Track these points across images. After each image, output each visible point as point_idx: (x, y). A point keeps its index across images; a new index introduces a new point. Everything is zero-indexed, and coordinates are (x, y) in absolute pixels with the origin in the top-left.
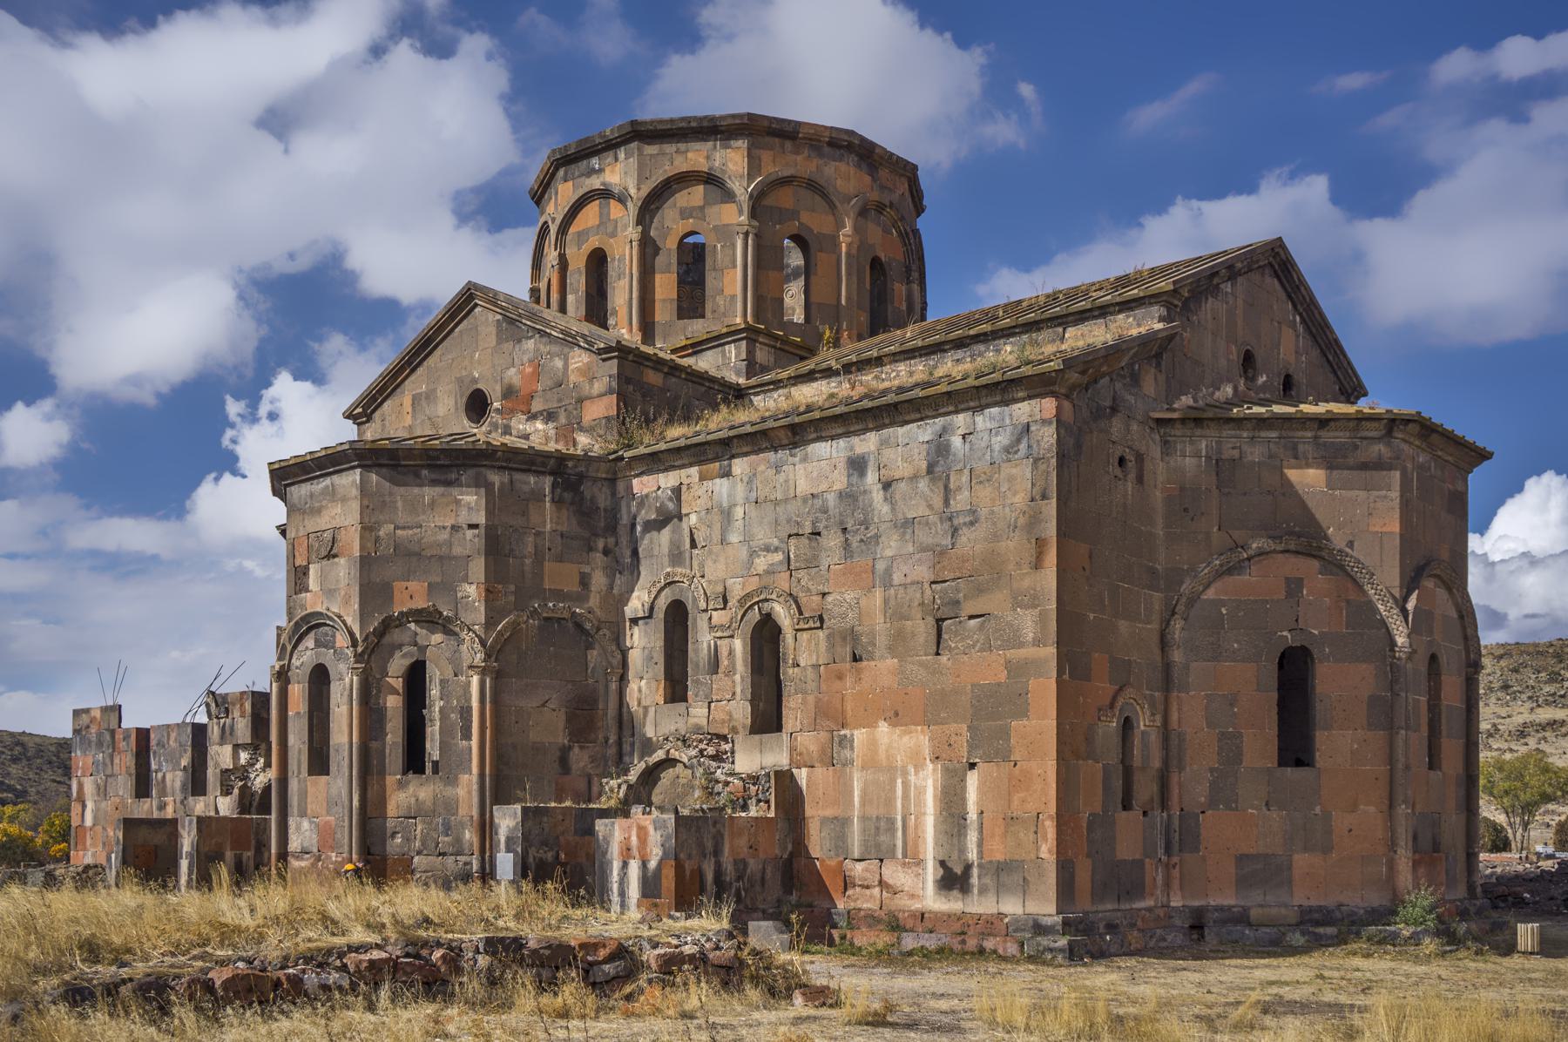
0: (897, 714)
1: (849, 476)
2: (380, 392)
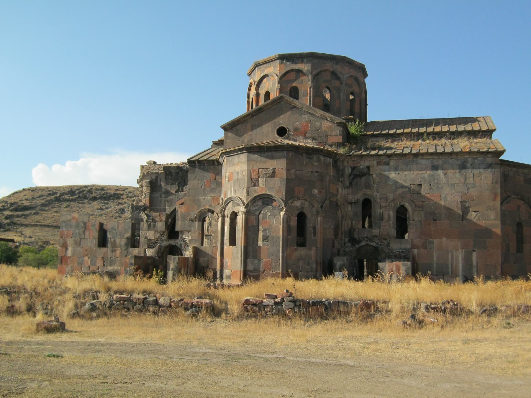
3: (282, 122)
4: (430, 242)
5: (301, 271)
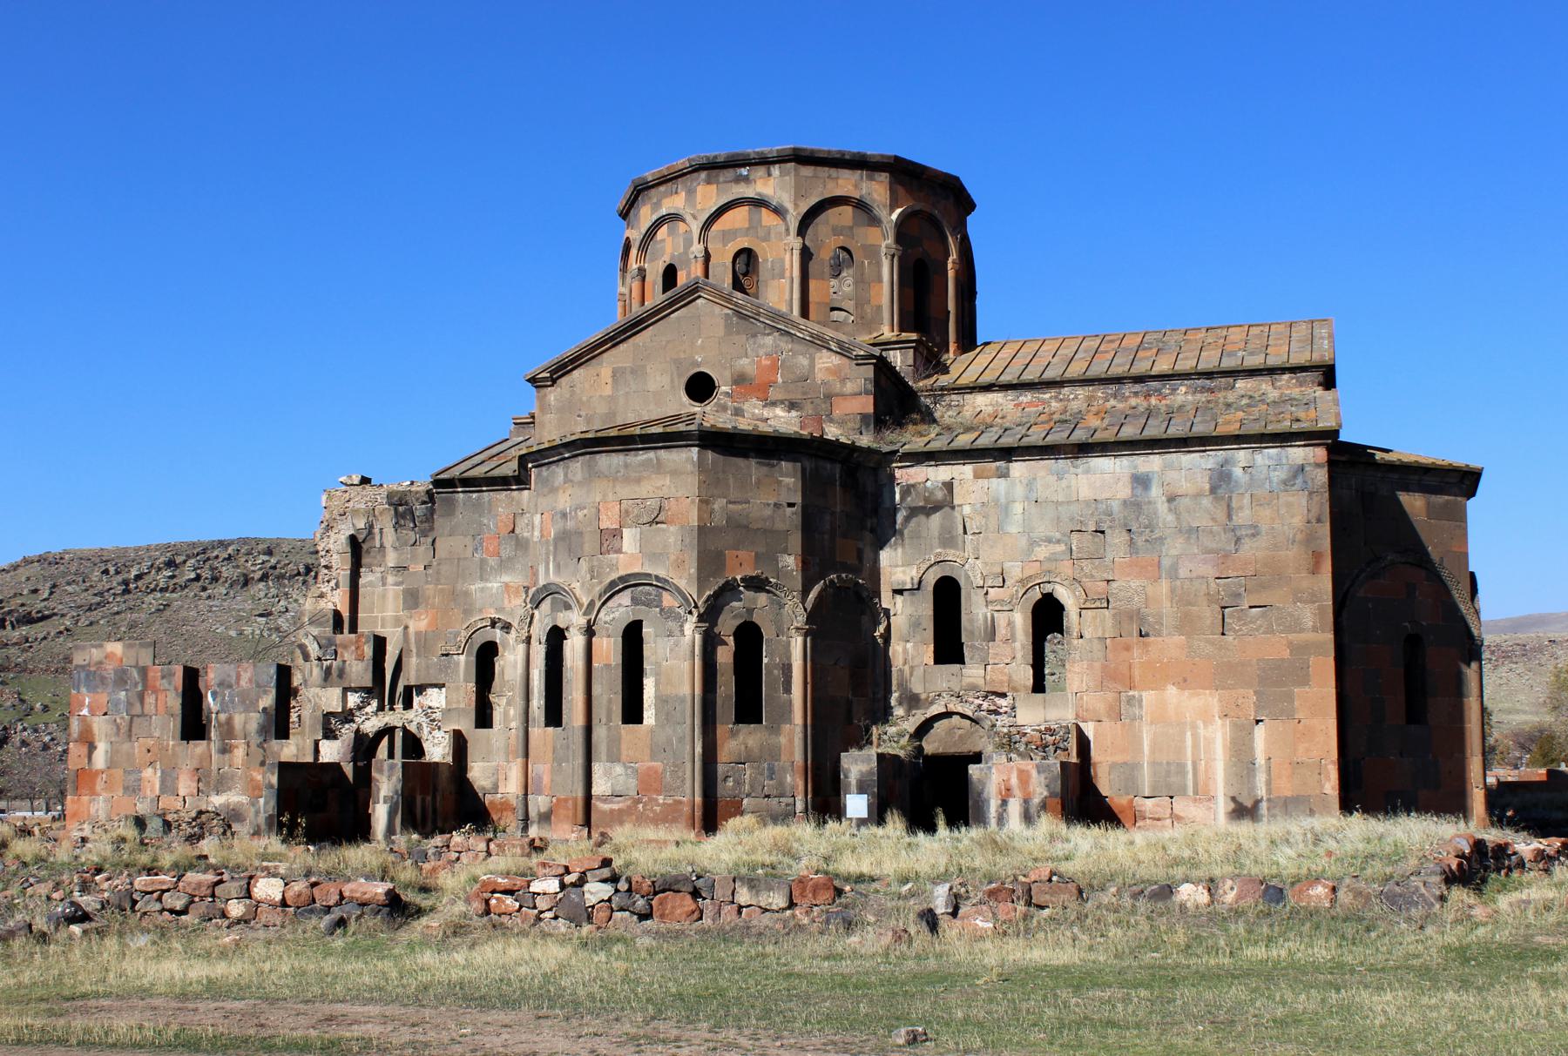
0: (1185, 681)
1: (1133, 488)
2: (572, 361)
3: (700, 360)
4: (1130, 700)
5: (748, 795)
